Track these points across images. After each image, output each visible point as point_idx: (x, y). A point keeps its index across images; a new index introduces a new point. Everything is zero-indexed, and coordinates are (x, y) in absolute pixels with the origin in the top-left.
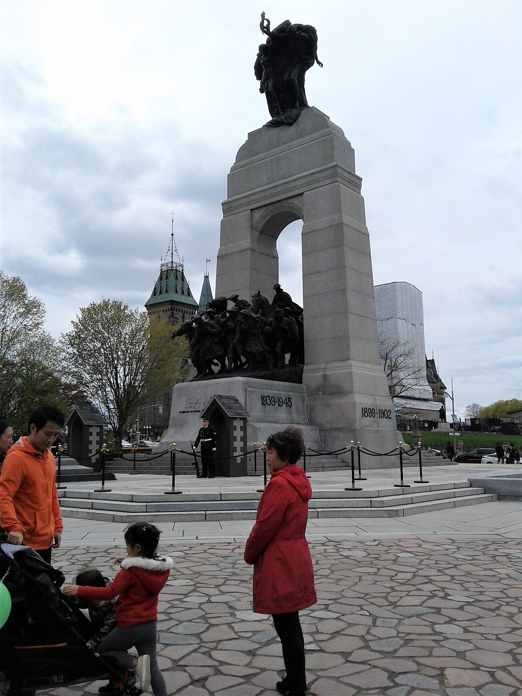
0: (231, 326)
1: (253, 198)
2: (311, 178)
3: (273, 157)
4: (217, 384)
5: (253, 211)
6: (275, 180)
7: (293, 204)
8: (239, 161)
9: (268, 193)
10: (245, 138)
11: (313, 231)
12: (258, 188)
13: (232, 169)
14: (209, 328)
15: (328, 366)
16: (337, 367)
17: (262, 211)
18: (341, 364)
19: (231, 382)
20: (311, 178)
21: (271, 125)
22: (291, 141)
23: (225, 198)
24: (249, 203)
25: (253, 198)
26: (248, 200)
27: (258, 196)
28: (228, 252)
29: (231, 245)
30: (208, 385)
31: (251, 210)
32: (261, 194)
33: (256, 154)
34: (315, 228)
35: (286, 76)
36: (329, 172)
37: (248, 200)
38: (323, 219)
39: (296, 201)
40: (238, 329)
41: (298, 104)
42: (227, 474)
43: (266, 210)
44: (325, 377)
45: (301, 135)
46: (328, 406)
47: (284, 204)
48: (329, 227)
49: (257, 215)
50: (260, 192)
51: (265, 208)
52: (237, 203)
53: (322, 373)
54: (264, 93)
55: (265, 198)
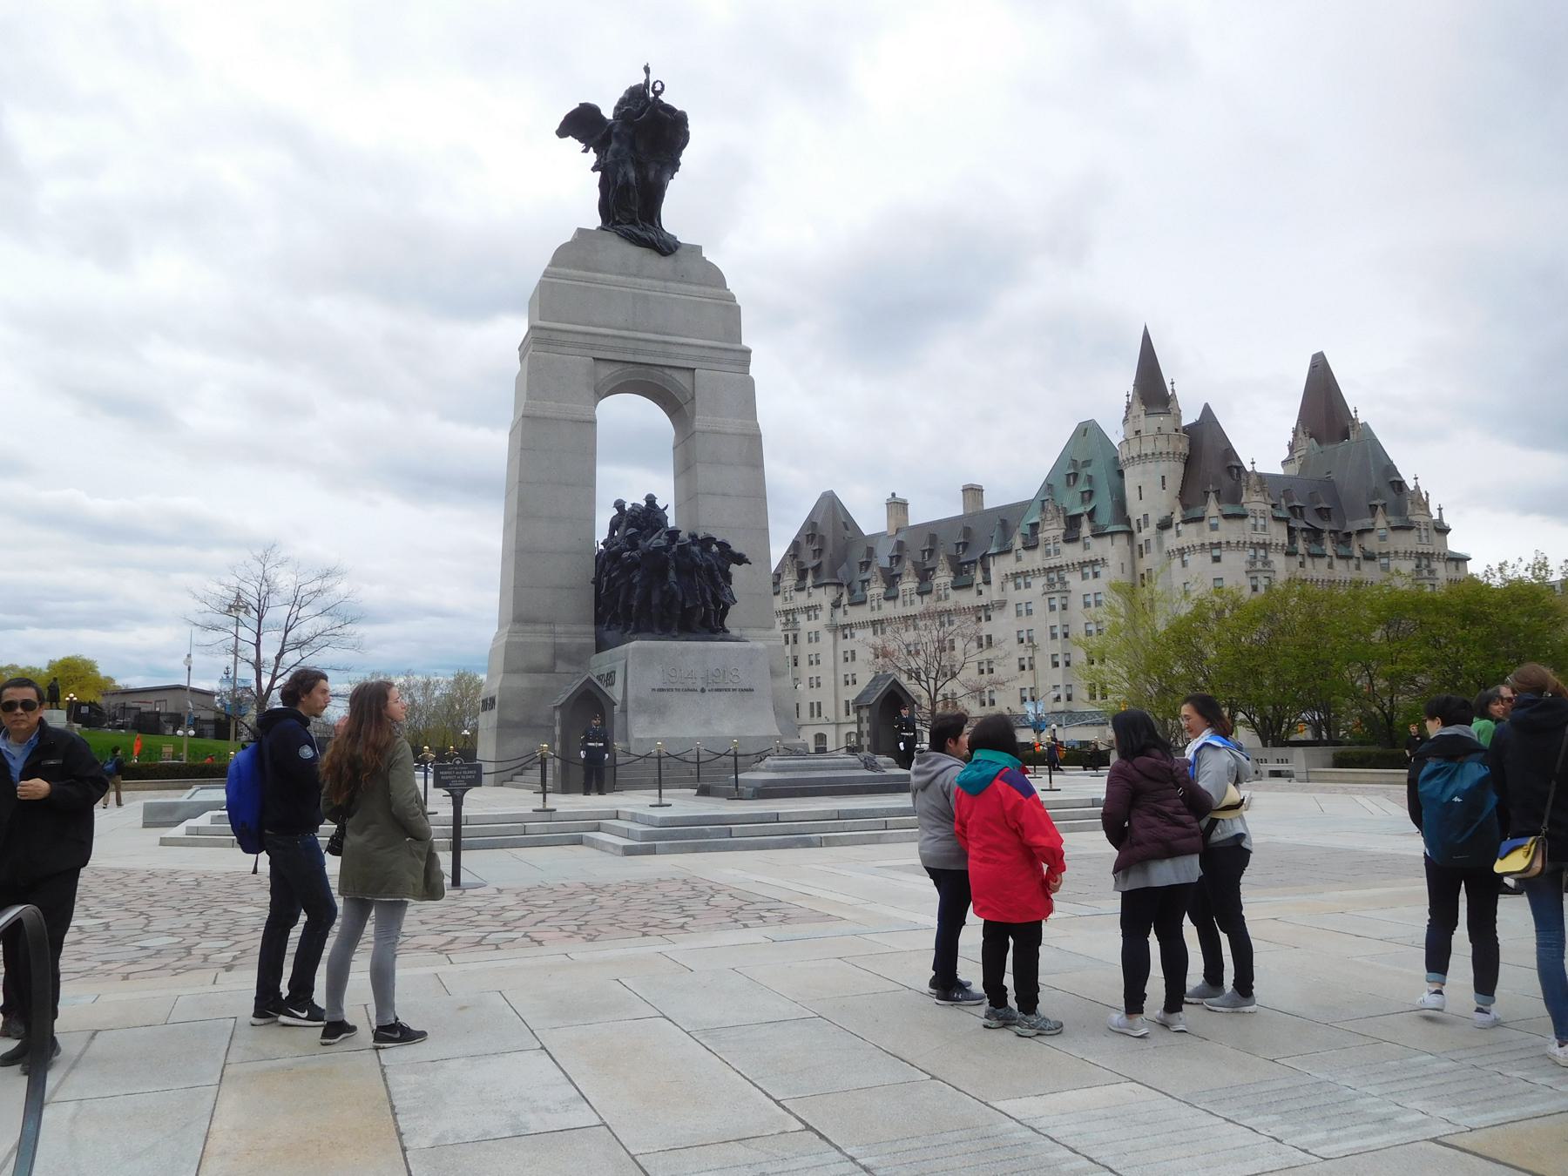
1: (600, 341)
2: (706, 353)
4: (726, 649)
9: (631, 345)
13: (546, 274)
18: (762, 632)
19: (752, 650)
20: (706, 353)
21: (601, 228)
22: (666, 280)
24: (592, 347)
25: (600, 341)
26: (588, 339)
35: (652, 174)
37: (588, 339)
39: (677, 375)
42: (612, 790)
45: (683, 278)
47: (654, 371)
49: (605, 371)
50: (614, 337)
51: (619, 366)
52: (564, 337)
55: (624, 350)
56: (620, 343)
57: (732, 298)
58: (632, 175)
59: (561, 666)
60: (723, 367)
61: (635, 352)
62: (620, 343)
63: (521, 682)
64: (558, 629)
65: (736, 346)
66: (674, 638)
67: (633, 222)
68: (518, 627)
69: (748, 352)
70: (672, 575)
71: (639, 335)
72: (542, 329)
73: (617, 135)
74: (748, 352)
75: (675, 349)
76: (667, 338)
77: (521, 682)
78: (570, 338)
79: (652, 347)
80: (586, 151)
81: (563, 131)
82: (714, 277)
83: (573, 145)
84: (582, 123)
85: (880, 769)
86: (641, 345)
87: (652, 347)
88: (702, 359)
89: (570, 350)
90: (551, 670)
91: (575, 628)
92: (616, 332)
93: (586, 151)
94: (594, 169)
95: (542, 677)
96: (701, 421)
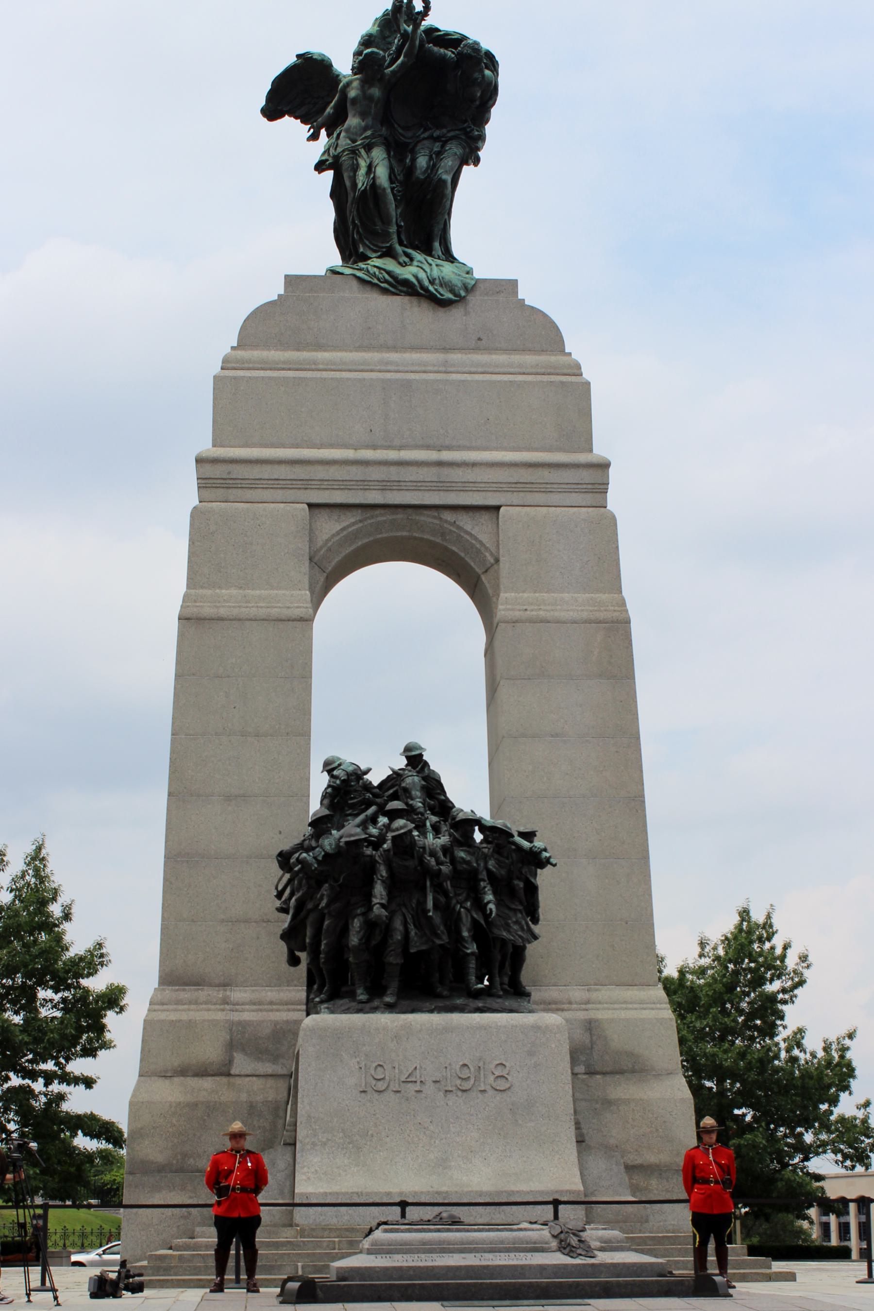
0: (468, 863)
1: (321, 473)
3: (388, 376)
5: (316, 511)
6: (397, 442)
7: (459, 527)
8: (255, 346)
9: (376, 474)
10: (275, 289)
11: (532, 621)
12: (332, 446)
13: (227, 364)
14: (433, 861)
15: (594, 995)
16: (625, 1002)
17: (350, 519)
19: (536, 1028)
22: (445, 350)
23: (203, 442)
24: (306, 484)
25: (321, 473)
26: (300, 472)
27: (334, 473)
28: (223, 612)
29: (234, 592)
30: (448, 1029)
31: (311, 506)
32: (354, 469)
33: (319, 347)
34: (541, 613)
35: (422, 162)
36: (586, 476)
37: (300, 472)
38: (566, 596)
39: (465, 522)
40: (484, 875)
41: (437, 245)
43: (360, 521)
44: (590, 1026)
45: (479, 345)
46: (608, 1103)
47: (425, 518)
48: (588, 621)
49: (330, 527)
51: (357, 515)
53: (582, 1015)
54: (329, 175)
56: (356, 473)
57: (576, 370)
58: (382, 173)
59: (242, 1063)
60: (555, 498)
61: (385, 486)
62: (356, 473)
63: (170, 1092)
64: (237, 995)
65: (582, 458)
66: (391, 1008)
67: (389, 253)
68: (169, 993)
69: (604, 466)
70: (379, 891)
71: (392, 455)
72: (215, 461)
73: (354, 101)
74: (604, 466)
75: (458, 475)
76: (446, 456)
77: (170, 1092)
78: (266, 472)
79: (412, 474)
80: (314, 137)
81: (273, 109)
82: (543, 334)
83: (292, 128)
84: (303, 90)
85: (589, 1252)
86: (394, 473)
87: (412, 474)
88: (517, 487)
89: (267, 494)
90: (224, 1071)
91: (271, 994)
92: (350, 454)
93: (314, 137)
94: (320, 167)
95: (207, 1083)
96: (507, 604)
